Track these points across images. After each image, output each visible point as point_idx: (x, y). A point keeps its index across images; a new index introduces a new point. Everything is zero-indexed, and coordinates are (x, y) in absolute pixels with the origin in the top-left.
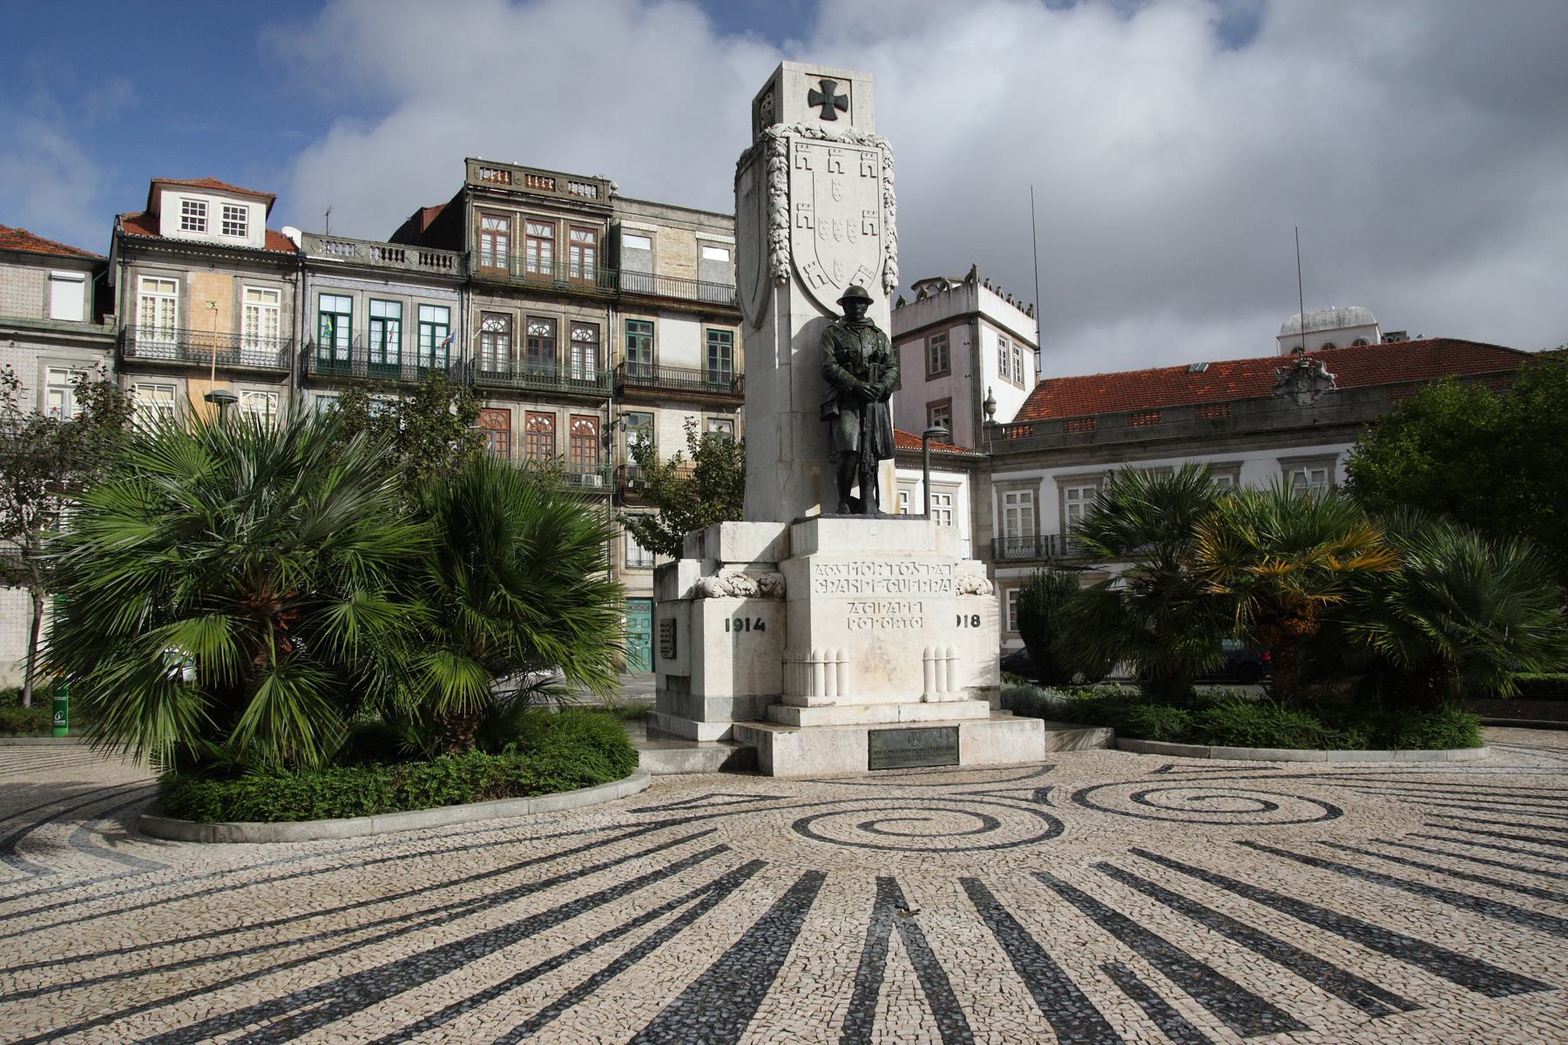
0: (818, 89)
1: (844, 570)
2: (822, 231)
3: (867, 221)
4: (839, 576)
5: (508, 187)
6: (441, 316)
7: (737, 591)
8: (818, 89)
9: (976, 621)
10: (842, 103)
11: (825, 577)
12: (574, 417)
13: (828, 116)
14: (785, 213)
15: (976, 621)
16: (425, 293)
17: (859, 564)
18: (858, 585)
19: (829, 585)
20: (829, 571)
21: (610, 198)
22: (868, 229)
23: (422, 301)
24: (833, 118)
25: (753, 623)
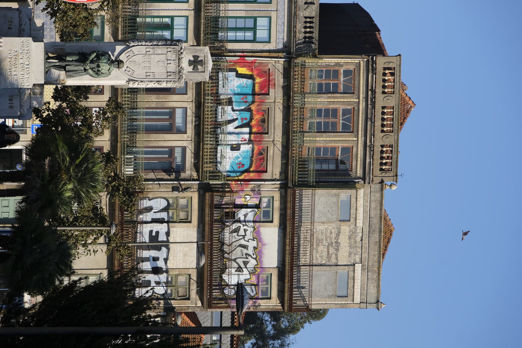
0: (199, 59)
1: (27, 49)
2: (145, 57)
3: (151, 74)
4: (25, 47)
5: (379, 90)
6: (262, 34)
7: (21, 22)
8: (199, 59)
9: (11, 107)
10: (195, 69)
11: (25, 42)
12: (184, 149)
13: (190, 63)
14: (151, 44)
15: (11, 107)
16: (280, 22)
17: (29, 54)
18: (23, 54)
19: (23, 44)
20: (27, 44)
21: (382, 182)
22: (148, 74)
23: (274, 20)
24: (190, 65)
25: (10, 27)
